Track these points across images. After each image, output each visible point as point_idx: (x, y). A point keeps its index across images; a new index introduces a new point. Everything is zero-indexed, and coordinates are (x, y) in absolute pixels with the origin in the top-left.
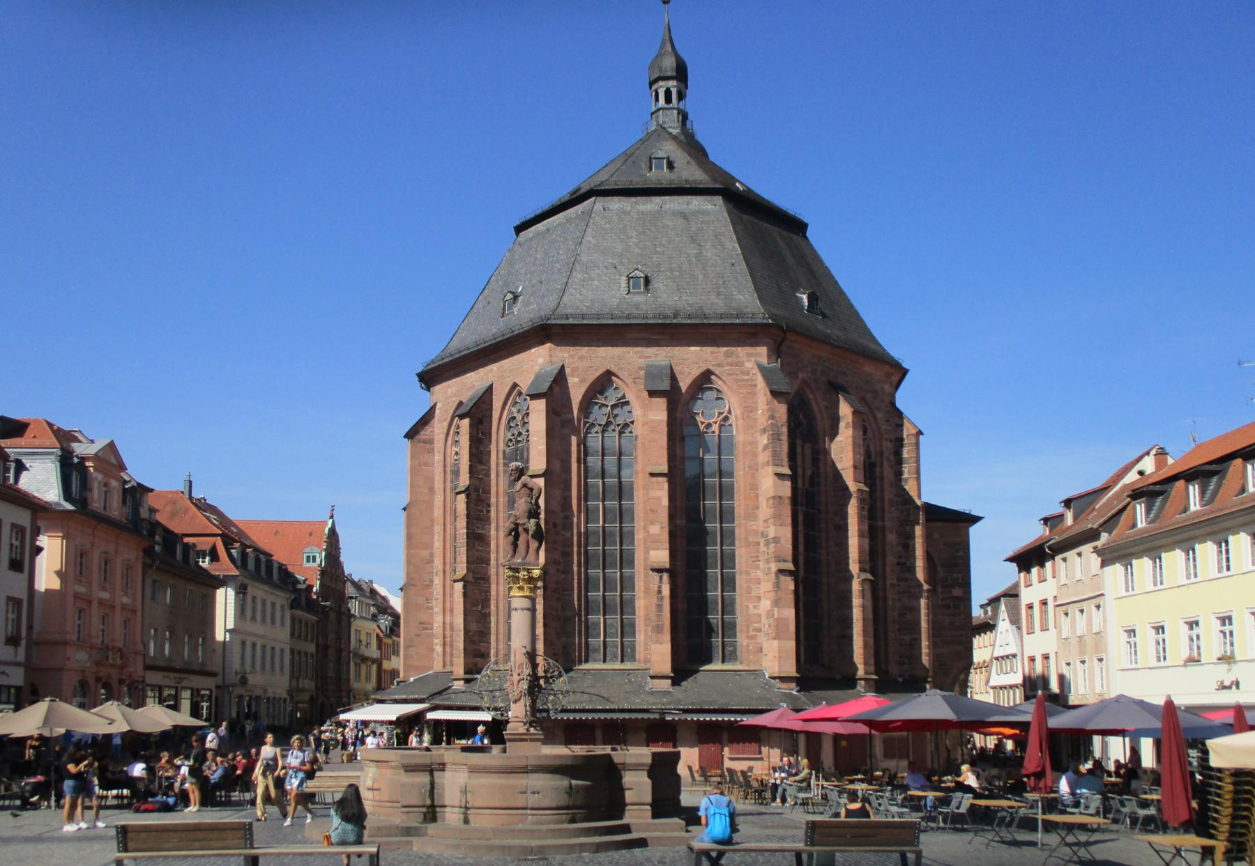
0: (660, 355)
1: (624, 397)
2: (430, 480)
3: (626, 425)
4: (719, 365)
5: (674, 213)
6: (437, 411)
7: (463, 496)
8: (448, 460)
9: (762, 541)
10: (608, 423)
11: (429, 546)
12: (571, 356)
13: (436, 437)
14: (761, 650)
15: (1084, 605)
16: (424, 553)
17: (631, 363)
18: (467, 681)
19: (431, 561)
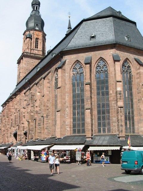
0: (137, 57)
1: (129, 65)
2: (65, 80)
3: (130, 72)
5: (128, 25)
6: (67, 62)
7: (89, 85)
8: (71, 75)
10: (127, 71)
11: (64, 99)
12: (120, 53)
13: (66, 69)
16: (64, 101)
17: (132, 57)
18: (92, 138)
19: (65, 104)
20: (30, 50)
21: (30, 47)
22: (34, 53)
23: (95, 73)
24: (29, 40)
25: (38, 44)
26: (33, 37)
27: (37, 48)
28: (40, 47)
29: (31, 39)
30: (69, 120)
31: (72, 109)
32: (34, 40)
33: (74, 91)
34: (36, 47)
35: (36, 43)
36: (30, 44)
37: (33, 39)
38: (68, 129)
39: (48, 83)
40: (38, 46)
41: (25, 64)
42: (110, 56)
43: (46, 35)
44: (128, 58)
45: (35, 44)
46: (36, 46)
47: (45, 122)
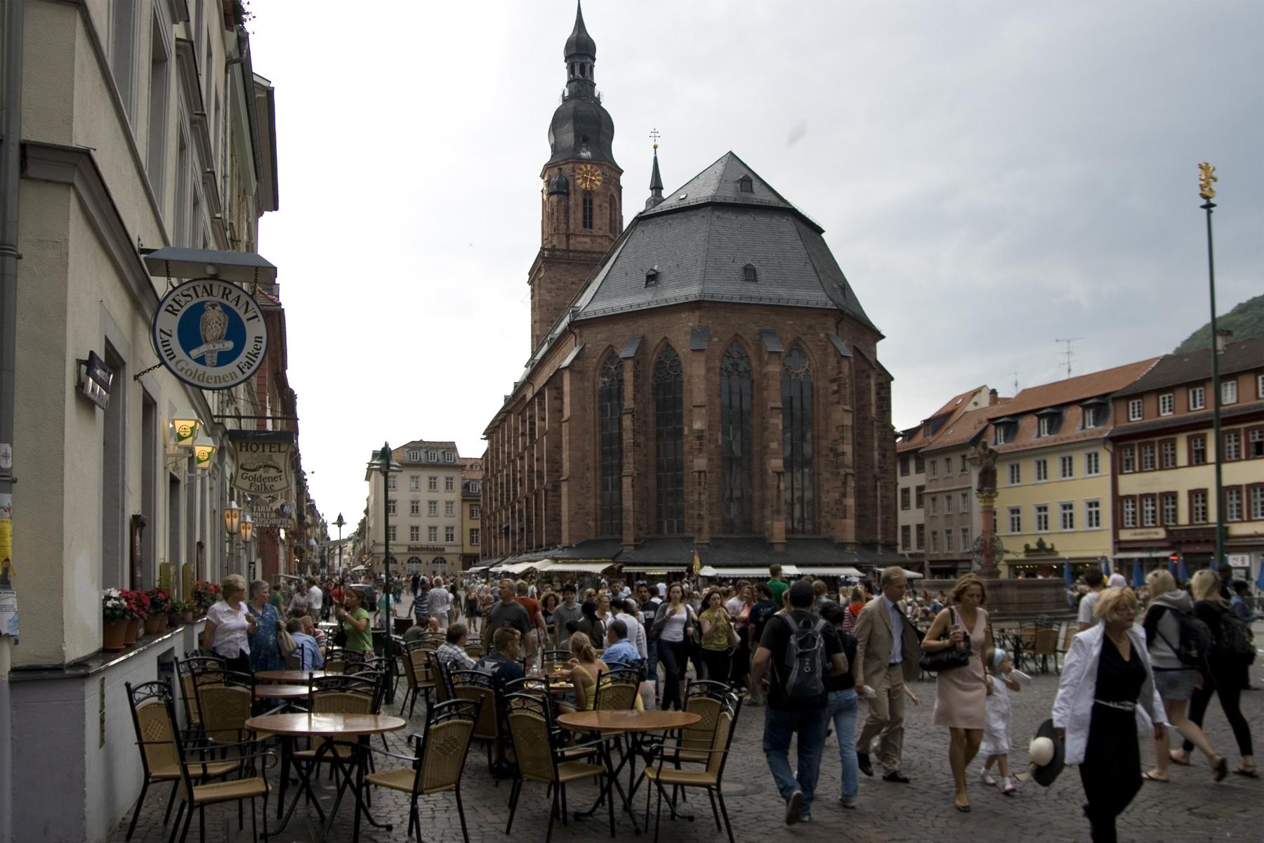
4: (805, 334)
9: (831, 455)
14: (829, 525)
15: (953, 494)
20: (564, 238)
21: (563, 226)
22: (580, 247)
23: (651, 380)
24: (559, 202)
25: (591, 210)
26: (571, 187)
27: (591, 227)
28: (600, 220)
29: (568, 194)
30: (592, 502)
31: (599, 474)
32: (575, 200)
33: (603, 426)
34: (585, 226)
35: (585, 209)
36: (562, 217)
37: (572, 196)
38: (591, 523)
39: (556, 398)
40: (591, 217)
41: (549, 291)
42: (686, 333)
43: (621, 172)
44: (740, 333)
45: (580, 215)
46: (588, 222)
47: (550, 504)
